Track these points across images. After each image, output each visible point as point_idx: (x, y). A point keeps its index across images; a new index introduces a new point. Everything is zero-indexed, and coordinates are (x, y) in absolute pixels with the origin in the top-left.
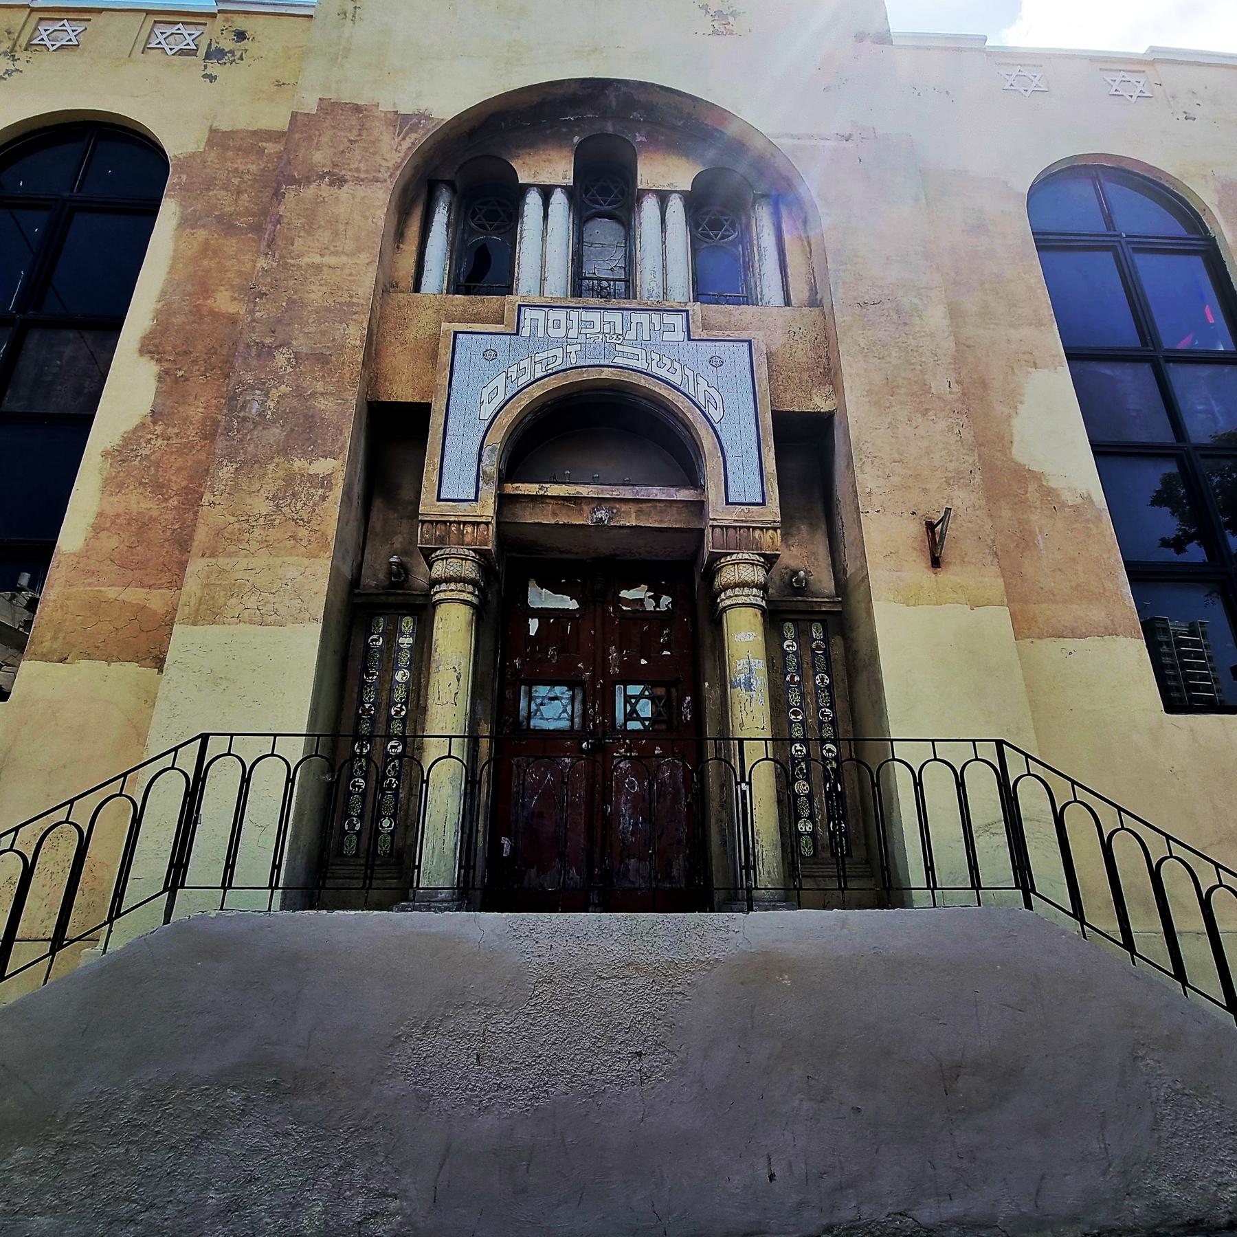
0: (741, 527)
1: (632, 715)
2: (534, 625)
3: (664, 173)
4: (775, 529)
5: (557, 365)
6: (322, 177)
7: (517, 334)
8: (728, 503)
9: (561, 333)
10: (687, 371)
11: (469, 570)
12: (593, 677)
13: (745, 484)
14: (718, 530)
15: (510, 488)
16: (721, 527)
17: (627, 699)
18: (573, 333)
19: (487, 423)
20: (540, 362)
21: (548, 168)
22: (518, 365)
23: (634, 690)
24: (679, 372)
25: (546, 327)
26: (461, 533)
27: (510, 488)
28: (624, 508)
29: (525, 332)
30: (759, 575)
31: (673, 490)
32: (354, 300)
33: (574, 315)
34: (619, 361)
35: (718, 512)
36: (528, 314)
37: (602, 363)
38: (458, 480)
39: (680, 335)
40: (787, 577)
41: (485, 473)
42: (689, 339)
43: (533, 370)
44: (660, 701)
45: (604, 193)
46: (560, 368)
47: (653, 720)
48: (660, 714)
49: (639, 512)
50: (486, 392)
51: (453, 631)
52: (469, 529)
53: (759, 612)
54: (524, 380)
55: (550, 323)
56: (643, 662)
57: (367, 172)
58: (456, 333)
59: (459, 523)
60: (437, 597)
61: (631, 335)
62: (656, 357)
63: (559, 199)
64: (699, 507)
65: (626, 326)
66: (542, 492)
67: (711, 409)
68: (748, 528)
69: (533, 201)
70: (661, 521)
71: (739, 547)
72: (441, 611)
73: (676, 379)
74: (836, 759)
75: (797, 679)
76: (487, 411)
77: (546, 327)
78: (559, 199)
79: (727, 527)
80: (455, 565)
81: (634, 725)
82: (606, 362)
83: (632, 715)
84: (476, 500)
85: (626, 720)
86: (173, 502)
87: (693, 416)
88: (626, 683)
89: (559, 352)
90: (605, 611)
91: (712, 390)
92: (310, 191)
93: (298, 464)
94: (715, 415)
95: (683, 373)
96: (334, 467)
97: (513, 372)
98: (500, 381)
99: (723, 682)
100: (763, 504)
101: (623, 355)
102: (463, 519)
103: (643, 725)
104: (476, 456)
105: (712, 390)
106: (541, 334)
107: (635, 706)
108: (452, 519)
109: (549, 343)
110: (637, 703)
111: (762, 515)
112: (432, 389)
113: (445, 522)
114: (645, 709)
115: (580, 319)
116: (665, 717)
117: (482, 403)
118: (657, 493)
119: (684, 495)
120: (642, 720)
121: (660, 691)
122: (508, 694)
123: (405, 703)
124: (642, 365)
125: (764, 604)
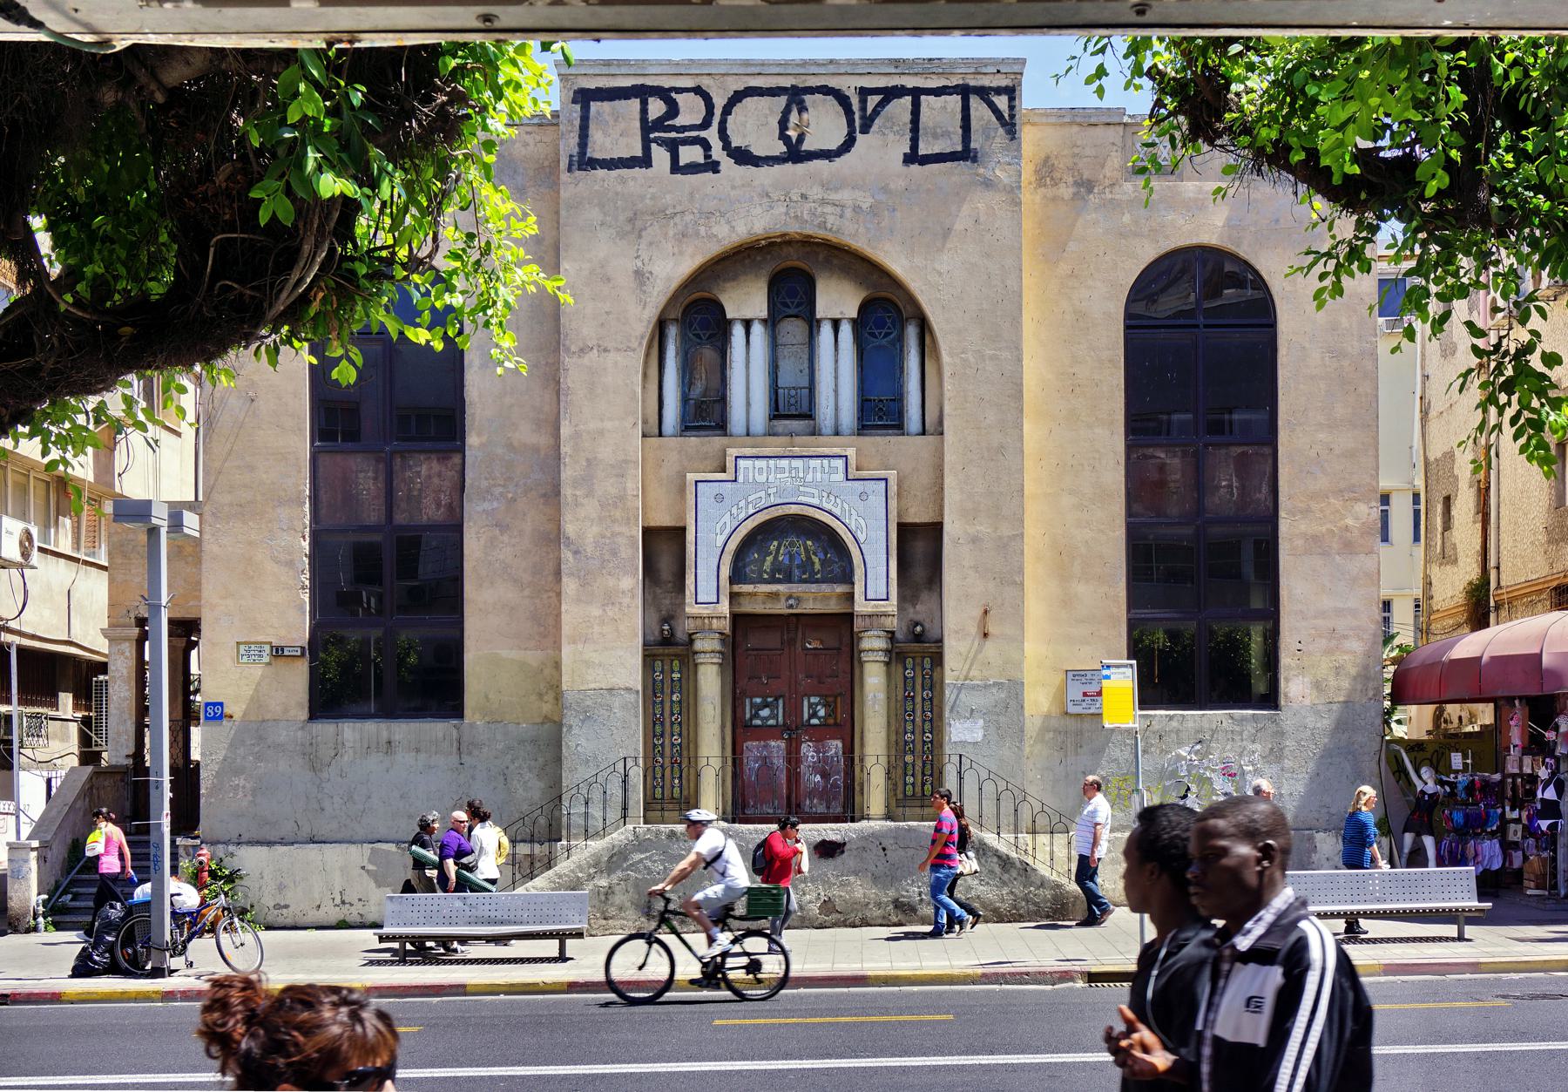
1: (814, 715)
3: (837, 300)
5: (761, 505)
11: (717, 646)
13: (877, 587)
15: (736, 588)
21: (746, 301)
23: (814, 700)
27: (736, 588)
29: (741, 479)
30: (881, 644)
33: (772, 462)
35: (861, 606)
38: (707, 594)
39: (841, 476)
45: (792, 298)
51: (710, 681)
54: (742, 516)
61: (809, 478)
63: (757, 329)
64: (850, 597)
65: (806, 469)
69: (738, 331)
72: (702, 669)
73: (837, 511)
76: (720, 543)
78: (757, 329)
80: (707, 645)
81: (815, 721)
86: (527, 592)
92: (586, 360)
93: (611, 582)
94: (862, 538)
96: (631, 582)
97: (734, 510)
98: (727, 518)
101: (805, 494)
107: (814, 709)
112: (683, 517)
118: (825, 587)
119: (840, 589)
124: (815, 501)
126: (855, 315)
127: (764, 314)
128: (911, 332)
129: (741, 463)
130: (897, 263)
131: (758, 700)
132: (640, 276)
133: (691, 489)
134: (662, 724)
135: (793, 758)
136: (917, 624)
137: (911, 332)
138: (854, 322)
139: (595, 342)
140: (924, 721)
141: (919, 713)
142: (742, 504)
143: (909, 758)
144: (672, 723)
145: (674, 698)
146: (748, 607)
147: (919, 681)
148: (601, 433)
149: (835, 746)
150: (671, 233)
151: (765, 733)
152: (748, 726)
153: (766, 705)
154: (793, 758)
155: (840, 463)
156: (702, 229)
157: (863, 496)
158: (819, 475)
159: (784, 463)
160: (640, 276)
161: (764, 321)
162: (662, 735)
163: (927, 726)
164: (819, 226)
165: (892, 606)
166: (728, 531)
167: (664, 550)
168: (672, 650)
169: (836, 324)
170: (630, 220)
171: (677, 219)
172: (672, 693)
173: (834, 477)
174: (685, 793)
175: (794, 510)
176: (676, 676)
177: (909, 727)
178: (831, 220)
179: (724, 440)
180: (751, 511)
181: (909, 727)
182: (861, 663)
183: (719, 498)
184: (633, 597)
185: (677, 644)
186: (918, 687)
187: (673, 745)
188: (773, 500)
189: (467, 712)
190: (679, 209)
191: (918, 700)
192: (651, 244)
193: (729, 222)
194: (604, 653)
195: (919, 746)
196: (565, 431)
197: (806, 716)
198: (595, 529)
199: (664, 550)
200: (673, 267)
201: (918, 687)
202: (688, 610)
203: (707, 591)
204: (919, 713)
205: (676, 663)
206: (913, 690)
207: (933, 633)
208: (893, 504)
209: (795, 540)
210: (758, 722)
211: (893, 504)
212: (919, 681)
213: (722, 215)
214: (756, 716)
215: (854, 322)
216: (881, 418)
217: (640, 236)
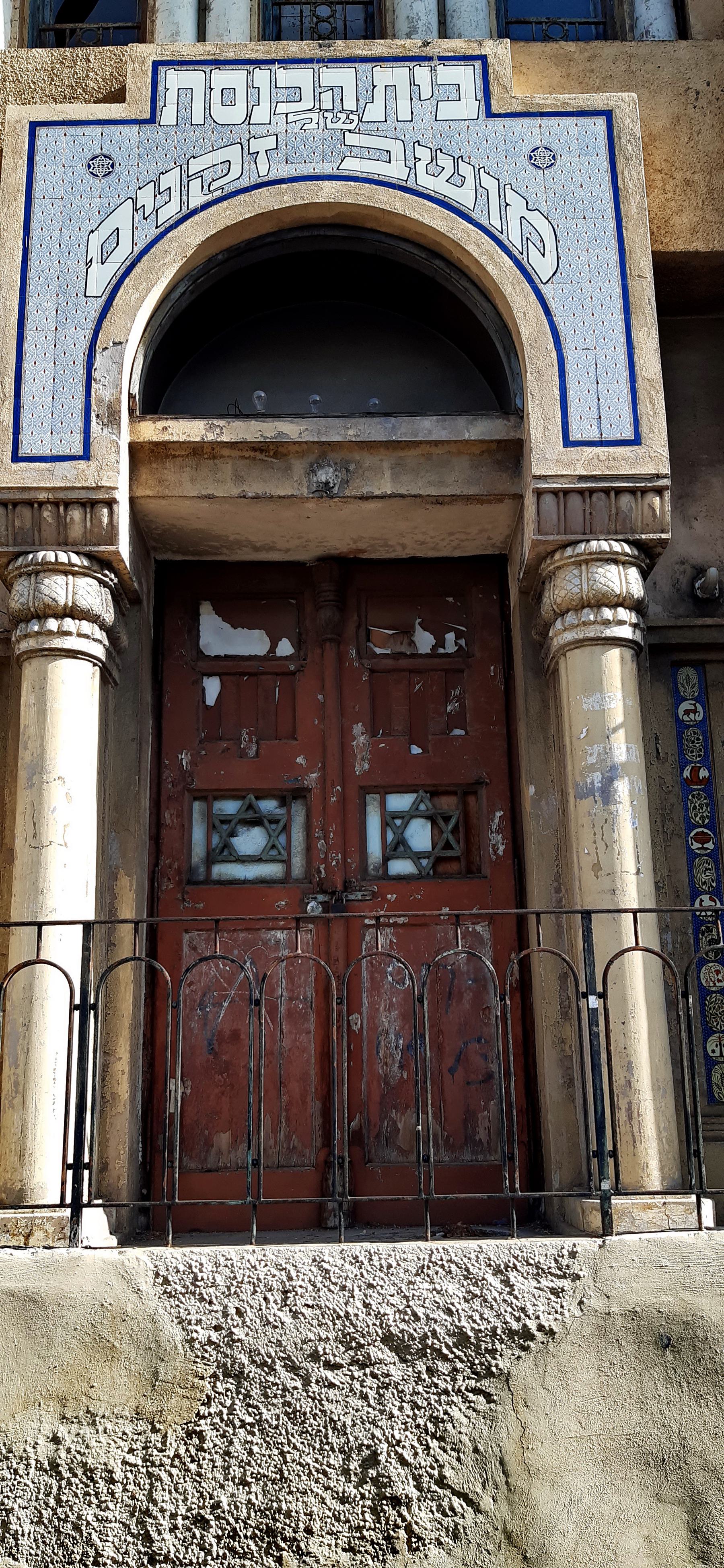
0: (592, 491)
1: (397, 847)
2: (212, 688)
4: (659, 491)
5: (234, 178)
7: (152, 120)
9: (237, 114)
10: (488, 182)
12: (323, 780)
14: (548, 499)
16: (555, 492)
17: (388, 820)
18: (261, 114)
19: (101, 302)
20: (200, 174)
22: (157, 182)
23: (399, 802)
24: (470, 182)
25: (208, 107)
26: (62, 525)
28: (368, 460)
29: (168, 116)
30: (627, 581)
31: (461, 421)
33: (261, 76)
34: (352, 165)
36: (173, 79)
37: (318, 172)
39: (469, 106)
40: (684, 581)
41: (100, 401)
42: (490, 115)
43: (184, 188)
44: (447, 819)
46: (237, 185)
47: (438, 860)
48: (448, 846)
49: (398, 469)
50: (96, 240)
52: (76, 514)
53: (628, 653)
54: (170, 211)
55: (216, 95)
56: (416, 750)
58: (34, 126)
59: (56, 504)
60: (24, 646)
61: (375, 112)
62: (424, 154)
64: (512, 453)
66: (210, 437)
67: (534, 253)
68: (606, 491)
70: (442, 483)
71: (590, 532)
73: (464, 197)
75: (704, 773)
76: (99, 279)
77: (208, 107)
79: (566, 492)
81: (401, 867)
82: (327, 168)
83: (397, 847)
84: (86, 456)
85: (386, 859)
87: (499, 270)
88: (385, 790)
89: (234, 153)
90: (341, 658)
91: (535, 218)
94: (543, 266)
95: (478, 184)
97: (146, 197)
98: (123, 218)
99: (558, 783)
100: (637, 441)
102: (61, 495)
103: (417, 864)
104: (81, 371)
105: (535, 218)
106: (198, 119)
107: (401, 831)
108: (42, 496)
110: (406, 825)
111: (637, 460)
113: (30, 503)
114: (420, 836)
115: (274, 85)
116: (457, 850)
117: (89, 263)
118: (428, 427)
120: (417, 857)
121: (448, 803)
124: (395, 171)
125: (638, 637)
131: (230, 807)
135: (337, 992)
142: (171, 180)
152: (194, 881)
153: (256, 822)
157: (542, 158)
166: (124, 252)
173: (447, 110)
175: (328, 192)
180: (197, 199)
183: (102, 165)
214: (224, 852)
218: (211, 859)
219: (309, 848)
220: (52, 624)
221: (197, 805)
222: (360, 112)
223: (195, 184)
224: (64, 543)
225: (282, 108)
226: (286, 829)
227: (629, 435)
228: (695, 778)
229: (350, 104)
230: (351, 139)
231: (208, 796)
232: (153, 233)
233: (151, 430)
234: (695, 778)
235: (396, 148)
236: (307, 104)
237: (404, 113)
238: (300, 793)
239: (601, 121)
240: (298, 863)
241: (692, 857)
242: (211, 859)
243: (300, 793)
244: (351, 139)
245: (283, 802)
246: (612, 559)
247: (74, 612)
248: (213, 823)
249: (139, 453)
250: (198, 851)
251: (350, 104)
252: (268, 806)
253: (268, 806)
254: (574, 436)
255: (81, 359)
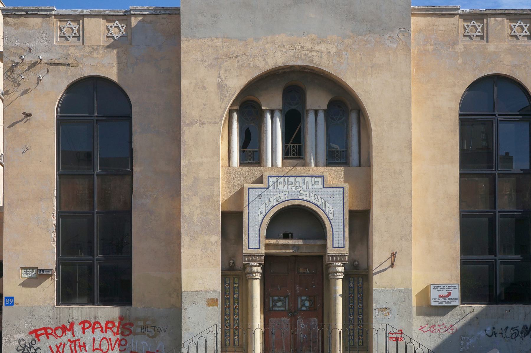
1: (303, 305)
3: (317, 100)
5: (281, 200)
6: (196, 122)
8: (333, 247)
10: (323, 201)
17: (302, 301)
18: (286, 187)
20: (276, 199)
23: (304, 298)
25: (277, 186)
29: (271, 188)
31: (317, 241)
32: (215, 176)
34: (301, 197)
35: (330, 250)
39: (320, 186)
42: (324, 188)
43: (274, 201)
50: (259, 210)
54: (271, 205)
57: (212, 119)
58: (249, 188)
61: (305, 187)
62: (313, 195)
64: (325, 246)
65: (303, 182)
73: (319, 203)
74: (362, 319)
76: (260, 217)
77: (277, 186)
81: (304, 308)
84: (259, 248)
89: (281, 195)
91: (330, 208)
93: (206, 238)
94: (331, 217)
95: (321, 201)
96: (216, 238)
97: (267, 203)
100: (344, 248)
105: (330, 208)
109: (279, 191)
114: (307, 304)
120: (306, 307)
122: (267, 300)
123: (238, 304)
124: (308, 198)
126: (325, 107)
127: (281, 107)
128: (353, 117)
129: (272, 180)
130: (350, 81)
131: (276, 298)
132: (221, 87)
133: (245, 192)
134: (229, 309)
136: (355, 261)
137: (353, 117)
138: (325, 111)
139: (198, 119)
140: (359, 308)
141: (356, 305)
142: (271, 199)
143: (351, 327)
144: (234, 309)
145: (235, 297)
146: (273, 251)
147: (356, 289)
148: (201, 164)
149: (314, 321)
150: (236, 65)
151: (279, 314)
154: (293, 326)
155: (320, 180)
156: (251, 63)
157: (332, 196)
158: (310, 185)
159: (292, 179)
160: (221, 87)
161: (281, 111)
162: (229, 315)
163: (360, 311)
164: (310, 61)
165: (346, 251)
167: (232, 221)
168: (232, 273)
169: (316, 112)
170: (215, 59)
171: (239, 58)
172: (234, 294)
173: (317, 187)
174: (240, 343)
175: (297, 202)
176: (236, 285)
177: (351, 312)
178: (315, 59)
179: (261, 168)
181: (351, 312)
182: (329, 280)
184: (217, 246)
185: (237, 270)
186: (356, 292)
187: (234, 319)
188: (287, 198)
189: (134, 302)
190: (240, 53)
191: (356, 298)
192: (226, 70)
193: (264, 60)
194: (201, 273)
195: (356, 320)
196: (183, 162)
197: (299, 306)
198: (198, 211)
199: (232, 221)
200: (237, 83)
201: (356, 292)
202: (244, 252)
203: (254, 244)
204: (356, 305)
205: (236, 279)
206: (353, 293)
207: (364, 265)
208: (347, 199)
209: (296, 219)
210: (277, 309)
211: (347, 199)
212: (356, 289)
213: (261, 56)
214: (275, 306)
215: (325, 111)
216: (337, 160)
217: (220, 67)
218: (273, 307)
219: (289, 305)
220: (254, 274)
221: (271, 298)
222: (302, 187)
223: (275, 200)
224: (256, 261)
225: (289, 186)
226: (285, 302)
227: (343, 246)
228: (351, 296)
229: (301, 185)
230: (301, 192)
231: (273, 297)
232: (269, 209)
233: (268, 242)
234: (351, 296)
235: (308, 194)
236: (293, 185)
237: (310, 188)
238: (287, 296)
239: (342, 189)
240: (287, 308)
241: (350, 308)
242: (273, 307)
243: (287, 296)
244: (301, 192)
245: (285, 297)
246: (339, 266)
247: (257, 272)
248: (273, 301)
249: (267, 246)
250: (271, 305)
251: (301, 185)
252: (282, 298)
253: (282, 298)
254: (334, 246)
255: (258, 232)
